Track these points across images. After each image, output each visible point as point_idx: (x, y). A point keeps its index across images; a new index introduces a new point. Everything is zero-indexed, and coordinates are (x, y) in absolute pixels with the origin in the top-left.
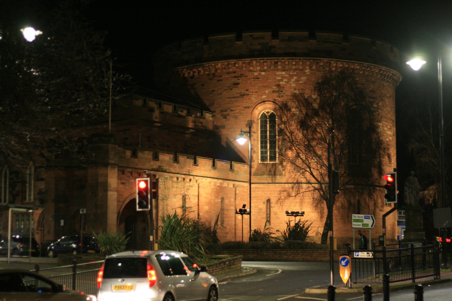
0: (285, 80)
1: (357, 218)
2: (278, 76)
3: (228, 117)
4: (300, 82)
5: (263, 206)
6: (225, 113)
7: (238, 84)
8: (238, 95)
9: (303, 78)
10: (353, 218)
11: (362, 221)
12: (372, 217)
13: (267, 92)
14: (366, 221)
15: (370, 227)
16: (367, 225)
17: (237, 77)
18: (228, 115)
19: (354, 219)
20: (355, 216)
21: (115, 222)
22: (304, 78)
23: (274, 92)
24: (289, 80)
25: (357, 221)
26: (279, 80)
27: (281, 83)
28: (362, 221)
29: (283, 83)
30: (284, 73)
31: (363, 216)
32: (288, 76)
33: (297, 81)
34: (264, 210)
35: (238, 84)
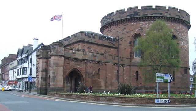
0: (143, 25)
1: (160, 76)
2: (141, 24)
4: (150, 26)
5: (135, 74)
7: (126, 28)
8: (126, 32)
9: (150, 24)
10: (157, 76)
11: (163, 78)
14: (166, 78)
15: (169, 81)
16: (167, 80)
18: (123, 40)
19: (157, 77)
20: (158, 75)
23: (139, 30)
25: (160, 78)
28: (163, 78)
31: (164, 74)
35: (126, 28)
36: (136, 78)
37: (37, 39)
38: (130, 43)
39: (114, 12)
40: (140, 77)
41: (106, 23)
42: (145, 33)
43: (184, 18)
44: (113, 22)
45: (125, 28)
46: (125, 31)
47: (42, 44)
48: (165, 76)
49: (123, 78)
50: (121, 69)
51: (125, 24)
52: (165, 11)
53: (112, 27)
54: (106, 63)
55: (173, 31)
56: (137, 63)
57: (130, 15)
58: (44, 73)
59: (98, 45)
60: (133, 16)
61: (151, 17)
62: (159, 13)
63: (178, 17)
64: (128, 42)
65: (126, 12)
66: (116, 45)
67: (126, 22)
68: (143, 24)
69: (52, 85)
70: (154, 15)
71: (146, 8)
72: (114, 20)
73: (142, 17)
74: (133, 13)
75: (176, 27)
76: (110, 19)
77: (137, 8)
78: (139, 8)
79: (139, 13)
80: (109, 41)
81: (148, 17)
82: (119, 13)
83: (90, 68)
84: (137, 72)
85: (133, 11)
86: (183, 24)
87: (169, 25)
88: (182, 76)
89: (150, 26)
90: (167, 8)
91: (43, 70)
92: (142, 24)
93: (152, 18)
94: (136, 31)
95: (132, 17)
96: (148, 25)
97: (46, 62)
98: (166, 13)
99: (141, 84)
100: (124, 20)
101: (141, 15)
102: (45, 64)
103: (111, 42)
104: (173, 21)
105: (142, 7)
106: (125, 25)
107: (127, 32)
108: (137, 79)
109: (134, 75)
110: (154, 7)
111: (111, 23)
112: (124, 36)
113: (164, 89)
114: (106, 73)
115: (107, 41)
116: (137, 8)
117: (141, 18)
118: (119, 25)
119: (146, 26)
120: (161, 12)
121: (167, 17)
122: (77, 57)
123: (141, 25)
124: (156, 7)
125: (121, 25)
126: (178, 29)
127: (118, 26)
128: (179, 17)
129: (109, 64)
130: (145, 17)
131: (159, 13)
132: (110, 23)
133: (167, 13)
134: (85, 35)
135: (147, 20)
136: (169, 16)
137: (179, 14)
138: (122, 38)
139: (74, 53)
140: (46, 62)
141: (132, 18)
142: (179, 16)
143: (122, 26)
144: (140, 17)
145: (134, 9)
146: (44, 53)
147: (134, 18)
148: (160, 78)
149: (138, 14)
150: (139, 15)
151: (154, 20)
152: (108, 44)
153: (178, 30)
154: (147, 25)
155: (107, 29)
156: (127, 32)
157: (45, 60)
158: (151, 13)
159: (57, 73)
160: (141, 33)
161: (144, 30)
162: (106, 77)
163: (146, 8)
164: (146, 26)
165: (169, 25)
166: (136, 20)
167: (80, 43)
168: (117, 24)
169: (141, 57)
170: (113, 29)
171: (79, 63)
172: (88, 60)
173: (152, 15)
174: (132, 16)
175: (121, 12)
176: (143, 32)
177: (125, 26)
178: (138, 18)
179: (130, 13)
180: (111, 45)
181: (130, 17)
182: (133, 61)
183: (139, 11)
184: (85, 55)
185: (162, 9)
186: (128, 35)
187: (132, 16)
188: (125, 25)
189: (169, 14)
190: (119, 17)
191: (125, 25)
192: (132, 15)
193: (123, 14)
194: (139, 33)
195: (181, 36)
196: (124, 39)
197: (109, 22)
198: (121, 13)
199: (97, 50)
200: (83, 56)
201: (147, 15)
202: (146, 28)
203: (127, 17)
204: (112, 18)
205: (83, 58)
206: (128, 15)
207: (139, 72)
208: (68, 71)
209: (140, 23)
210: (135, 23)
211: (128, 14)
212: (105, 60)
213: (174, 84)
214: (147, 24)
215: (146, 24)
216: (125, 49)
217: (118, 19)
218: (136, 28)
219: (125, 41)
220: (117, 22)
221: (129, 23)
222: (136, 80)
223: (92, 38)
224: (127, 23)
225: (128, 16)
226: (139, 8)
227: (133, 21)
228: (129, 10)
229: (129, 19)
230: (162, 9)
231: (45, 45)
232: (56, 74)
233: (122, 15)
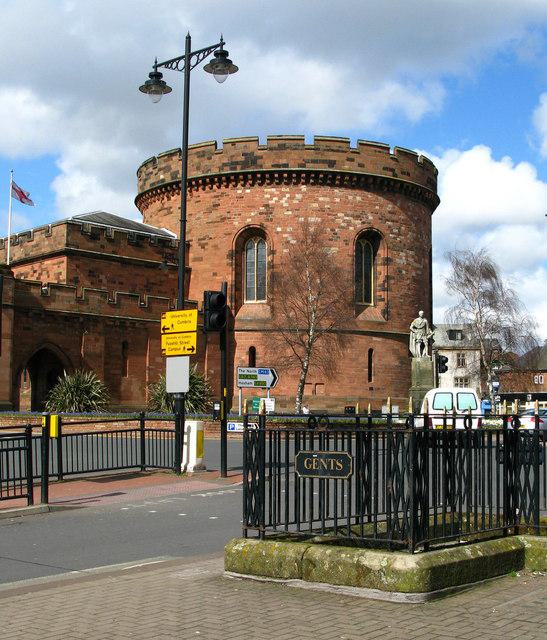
0: (275, 199)
11: (255, 377)
12: (272, 371)
17: (217, 196)
22: (299, 196)
25: (246, 377)
26: (268, 199)
28: (255, 377)
29: (273, 202)
30: (274, 190)
31: (257, 369)
41: (154, 183)
43: (408, 174)
46: (215, 215)
48: (260, 373)
52: (345, 156)
55: (371, 218)
56: (251, 321)
57: (232, 163)
60: (242, 169)
61: (299, 173)
62: (324, 162)
63: (389, 175)
68: (273, 195)
70: (310, 167)
71: (281, 144)
73: (272, 173)
74: (242, 158)
75: (381, 206)
76: (167, 169)
78: (263, 142)
79: (261, 158)
81: (290, 173)
82: (198, 152)
85: (241, 151)
86: (406, 194)
87: (359, 198)
88: (397, 363)
90: (354, 145)
92: (270, 193)
94: (252, 218)
98: (348, 159)
101: (267, 166)
104: (372, 186)
106: (215, 194)
107: (223, 219)
109: (243, 361)
110: (309, 141)
111: (171, 185)
113: (336, 406)
119: (284, 202)
120: (332, 158)
121: (351, 175)
123: (268, 196)
126: (389, 212)
128: (391, 173)
130: (281, 173)
131: (324, 162)
132: (165, 186)
133: (353, 160)
134: (84, 233)
137: (392, 164)
138: (204, 239)
141: (237, 175)
142: (392, 170)
144: (263, 173)
145: (244, 144)
147: (245, 175)
148: (246, 377)
149: (259, 162)
150: (261, 166)
153: (388, 216)
154: (285, 199)
158: (301, 161)
160: (266, 224)
164: (284, 202)
165: (359, 198)
167: (65, 259)
173: (304, 166)
174: (239, 167)
176: (272, 220)
177: (213, 200)
178: (259, 176)
179: (232, 156)
181: (231, 169)
183: (259, 153)
185: (335, 148)
186: (224, 228)
187: (239, 167)
188: (215, 197)
189: (361, 165)
190: (198, 168)
191: (215, 197)
192: (237, 163)
193: (210, 158)
194: (262, 225)
195: (399, 234)
196: (211, 243)
197: (163, 180)
198: (203, 156)
199: (123, 280)
200: (72, 303)
201: (286, 165)
203: (221, 169)
206: (224, 165)
207: (259, 350)
210: (248, 191)
211: (225, 161)
213: (371, 389)
215: (283, 195)
219: (216, 247)
226: (263, 142)
230: (335, 146)
233: (207, 162)
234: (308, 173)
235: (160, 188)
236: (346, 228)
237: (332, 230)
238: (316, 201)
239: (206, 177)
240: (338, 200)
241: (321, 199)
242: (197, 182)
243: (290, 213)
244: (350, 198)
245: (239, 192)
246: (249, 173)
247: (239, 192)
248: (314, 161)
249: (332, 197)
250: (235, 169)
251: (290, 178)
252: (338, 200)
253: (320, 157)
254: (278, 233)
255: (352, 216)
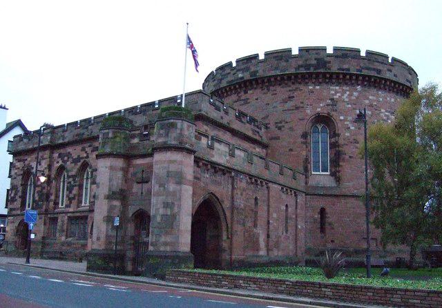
0: (339, 94)
3: (283, 129)
4: (353, 98)
5: (317, 216)
6: (279, 125)
9: (355, 93)
13: (321, 105)
21: (190, 228)
24: (342, 95)
27: (335, 97)
29: (337, 97)
30: (337, 88)
32: (341, 90)
33: (351, 95)
34: (319, 220)
35: (294, 97)
36: (319, 226)
37: (4, 108)
38: (305, 136)
39: (256, 56)
40: (330, 224)
42: (341, 114)
44: (256, 80)
45: (289, 97)
46: (290, 104)
47: (19, 123)
49: (296, 227)
50: (290, 200)
51: (290, 86)
53: (250, 92)
54: (270, 184)
56: (322, 187)
58: (117, 203)
59: (234, 133)
61: (357, 76)
62: (374, 69)
64: (300, 132)
65: (295, 57)
66: (265, 140)
67: (293, 83)
68: (337, 92)
69: (158, 242)
70: (365, 72)
71: (344, 54)
72: (260, 73)
74: (314, 62)
76: (243, 70)
77: (324, 49)
78: (330, 51)
79: (330, 62)
80: (252, 127)
81: (351, 75)
82: (278, 56)
83: (242, 195)
84: (322, 211)
85: (314, 56)
89: (353, 98)
91: (114, 193)
92: (335, 91)
93: (361, 78)
94: (321, 108)
95: (312, 70)
96: (349, 95)
97: (123, 169)
99: (332, 241)
100: (289, 77)
101: (334, 69)
102: (120, 174)
103: (257, 130)
105: (336, 49)
106: (291, 89)
107: (297, 108)
108: (322, 229)
111: (250, 81)
112: (288, 117)
114: (269, 211)
115: (248, 125)
116: (324, 49)
117: (334, 76)
118: (271, 88)
122: (216, 159)
124: (368, 53)
125: (279, 89)
127: (268, 90)
129: (276, 186)
130: (345, 75)
132: (245, 82)
135: (346, 84)
136: (394, 79)
138: (281, 122)
139: (211, 147)
140: (123, 169)
141: (310, 74)
143: (282, 92)
144: (331, 74)
146: (118, 139)
147: (318, 74)
149: (328, 65)
150: (330, 69)
151: (363, 85)
152: (250, 134)
154: (346, 95)
155: (234, 97)
156: (297, 108)
157: (120, 163)
158: (358, 68)
159: (179, 206)
161: (340, 106)
162: (269, 221)
163: (344, 52)
166: (320, 80)
168: (267, 86)
169: (328, 173)
170: (255, 97)
171: (219, 178)
172: (237, 171)
175: (281, 56)
176: (336, 111)
178: (328, 76)
180: (257, 137)
182: (312, 182)
183: (328, 59)
184: (232, 155)
188: (290, 91)
190: (276, 68)
192: (313, 65)
197: (242, 78)
198: (281, 59)
201: (348, 70)
202: (344, 101)
204: (253, 69)
205: (228, 165)
206: (302, 66)
207: (328, 210)
208: (201, 200)
209: (331, 87)
210: (318, 87)
211: (300, 63)
212: (266, 175)
214: (348, 93)
215: (344, 92)
216: (291, 150)
217: (273, 73)
218: (320, 100)
219: (291, 129)
220: (263, 82)
221: (301, 87)
222: (319, 231)
223: (222, 113)
224: (297, 85)
225: (301, 69)
226: (330, 51)
227: (314, 81)
228: (304, 52)
229: (303, 76)
230: (380, 59)
231: (56, 125)
232: (176, 209)
233: (284, 64)
234: (364, 76)
235: (239, 84)
236: (386, 121)
237: (378, 121)
238: (368, 99)
239: (285, 75)
240: (381, 100)
241: (370, 97)
242: (276, 79)
243: (350, 106)
244: (388, 99)
245: (311, 87)
246: (320, 73)
247: (311, 87)
248: (368, 69)
249: (378, 96)
250: (309, 69)
251: (351, 79)
252: (381, 100)
253: (371, 66)
254: (341, 120)
255: (389, 112)
